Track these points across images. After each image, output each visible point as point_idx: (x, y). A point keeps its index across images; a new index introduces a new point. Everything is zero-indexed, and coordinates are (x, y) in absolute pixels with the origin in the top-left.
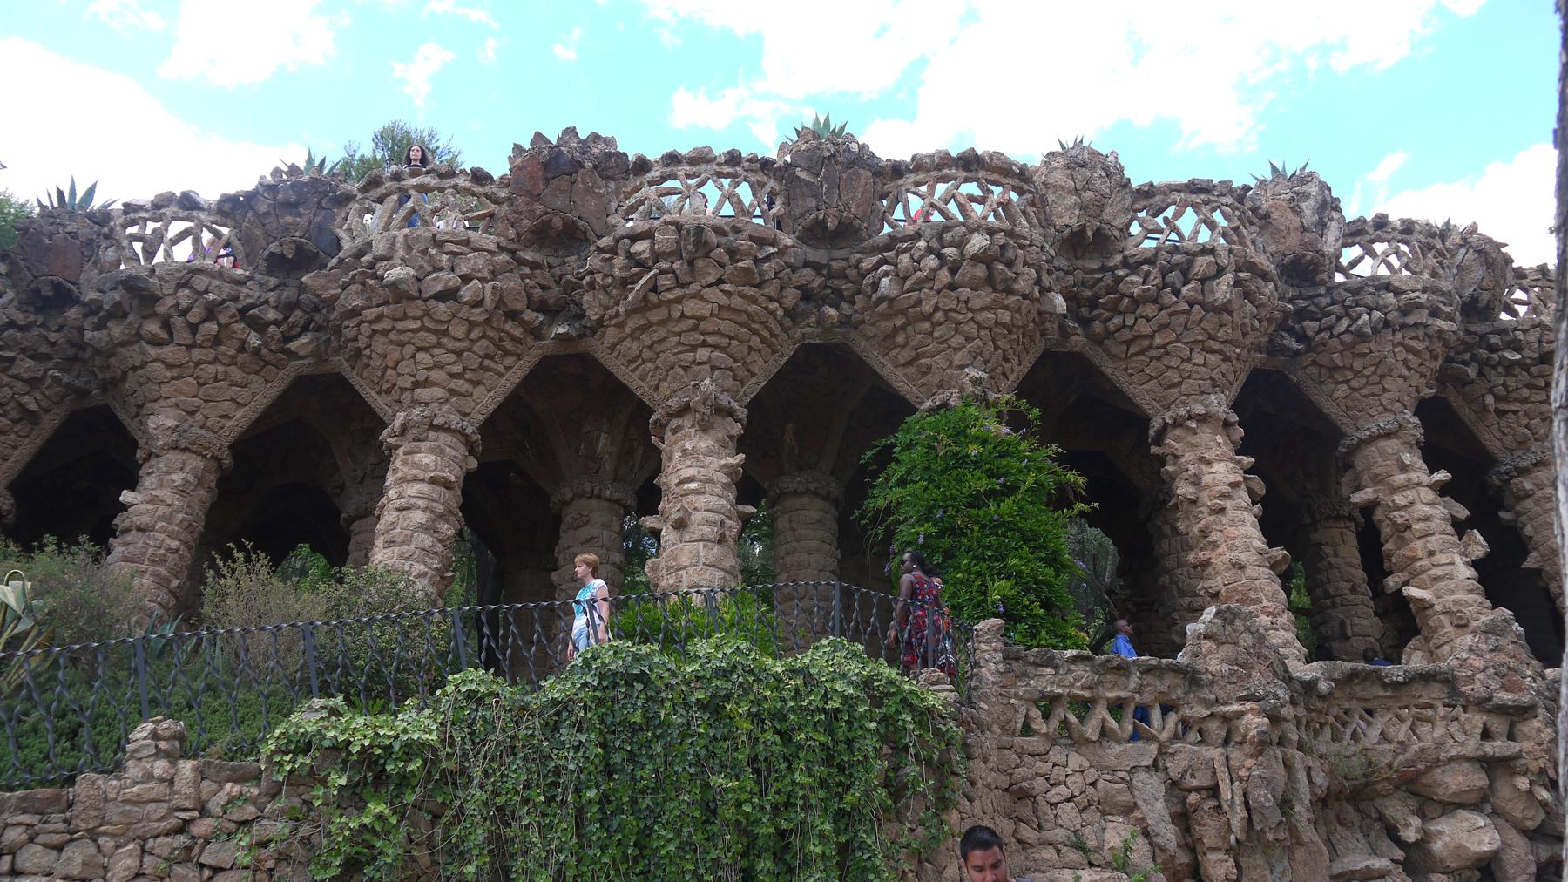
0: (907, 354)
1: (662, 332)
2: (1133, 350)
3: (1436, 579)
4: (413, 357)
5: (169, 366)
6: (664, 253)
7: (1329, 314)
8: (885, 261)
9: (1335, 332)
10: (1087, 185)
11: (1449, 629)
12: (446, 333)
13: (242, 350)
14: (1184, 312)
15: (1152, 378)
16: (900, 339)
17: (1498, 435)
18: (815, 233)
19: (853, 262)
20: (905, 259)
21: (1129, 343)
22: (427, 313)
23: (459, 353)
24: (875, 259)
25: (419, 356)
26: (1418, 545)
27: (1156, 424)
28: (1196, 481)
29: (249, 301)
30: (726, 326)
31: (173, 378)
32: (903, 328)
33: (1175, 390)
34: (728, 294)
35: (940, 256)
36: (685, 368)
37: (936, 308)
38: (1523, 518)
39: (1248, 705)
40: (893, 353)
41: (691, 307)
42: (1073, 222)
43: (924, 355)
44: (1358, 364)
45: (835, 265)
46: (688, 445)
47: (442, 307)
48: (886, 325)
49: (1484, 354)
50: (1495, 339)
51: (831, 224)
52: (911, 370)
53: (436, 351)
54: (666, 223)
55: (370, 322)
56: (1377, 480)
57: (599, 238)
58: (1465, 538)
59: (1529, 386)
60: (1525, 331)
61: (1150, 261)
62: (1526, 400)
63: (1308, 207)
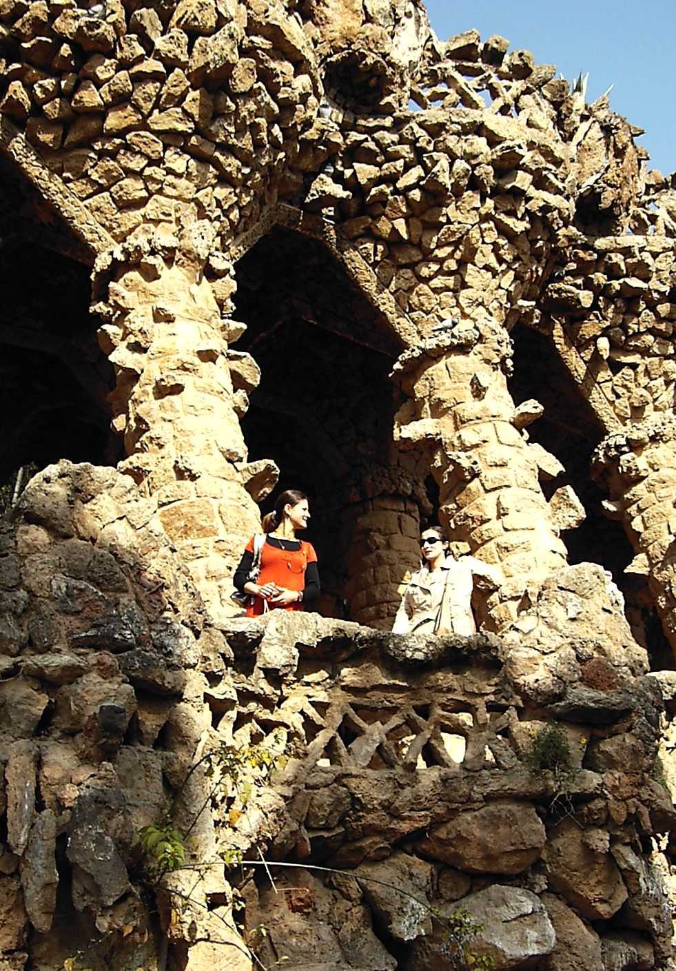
2: (71, 138)
9: (401, 184)
15: (101, 189)
17: (612, 397)
27: (102, 262)
38: (633, 510)
39: (93, 657)
49: (600, 278)
50: (617, 258)
58: (554, 499)
60: (655, 255)
62: (645, 352)
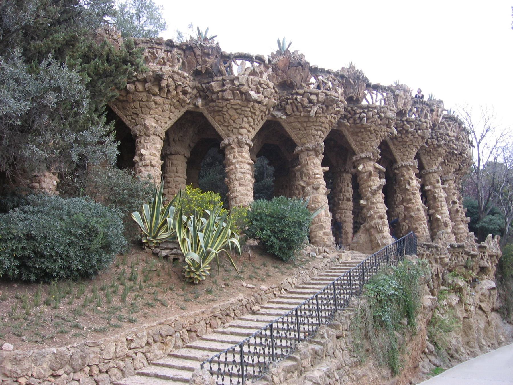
0: (360, 139)
1: (311, 124)
3: (442, 213)
4: (243, 119)
5: (156, 103)
6: (321, 102)
7: (433, 138)
8: (364, 112)
10: (406, 98)
11: (443, 227)
12: (255, 113)
13: (178, 101)
14: (417, 138)
16: (360, 134)
18: (350, 100)
19: (354, 109)
20: (370, 113)
21: (400, 142)
22: (253, 107)
23: (254, 119)
24: (362, 110)
25: (245, 119)
26: (439, 204)
28: (409, 184)
29: (186, 85)
30: (327, 126)
31: (156, 108)
32: (362, 132)
33: (406, 157)
34: (332, 117)
35: (380, 116)
36: (313, 136)
37: (374, 129)
40: (354, 137)
41: (323, 120)
42: (401, 107)
43: (364, 141)
44: (435, 153)
45: (349, 109)
46: (315, 162)
47: (257, 105)
48: (356, 130)
51: (355, 98)
52: (358, 143)
53: (250, 118)
54: (322, 92)
55: (231, 105)
56: (431, 184)
57: (298, 89)
59: (455, 160)
61: (412, 122)
63: (440, 110)
